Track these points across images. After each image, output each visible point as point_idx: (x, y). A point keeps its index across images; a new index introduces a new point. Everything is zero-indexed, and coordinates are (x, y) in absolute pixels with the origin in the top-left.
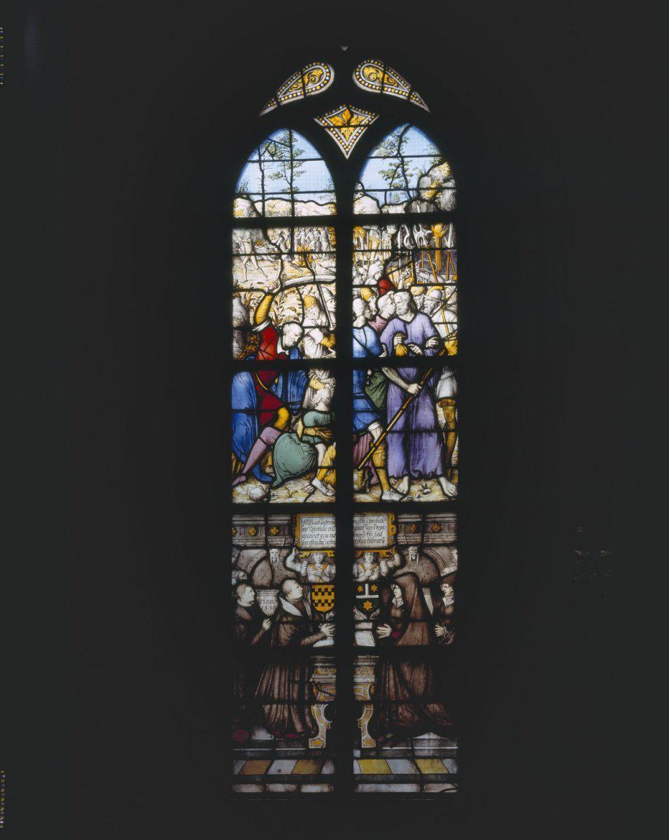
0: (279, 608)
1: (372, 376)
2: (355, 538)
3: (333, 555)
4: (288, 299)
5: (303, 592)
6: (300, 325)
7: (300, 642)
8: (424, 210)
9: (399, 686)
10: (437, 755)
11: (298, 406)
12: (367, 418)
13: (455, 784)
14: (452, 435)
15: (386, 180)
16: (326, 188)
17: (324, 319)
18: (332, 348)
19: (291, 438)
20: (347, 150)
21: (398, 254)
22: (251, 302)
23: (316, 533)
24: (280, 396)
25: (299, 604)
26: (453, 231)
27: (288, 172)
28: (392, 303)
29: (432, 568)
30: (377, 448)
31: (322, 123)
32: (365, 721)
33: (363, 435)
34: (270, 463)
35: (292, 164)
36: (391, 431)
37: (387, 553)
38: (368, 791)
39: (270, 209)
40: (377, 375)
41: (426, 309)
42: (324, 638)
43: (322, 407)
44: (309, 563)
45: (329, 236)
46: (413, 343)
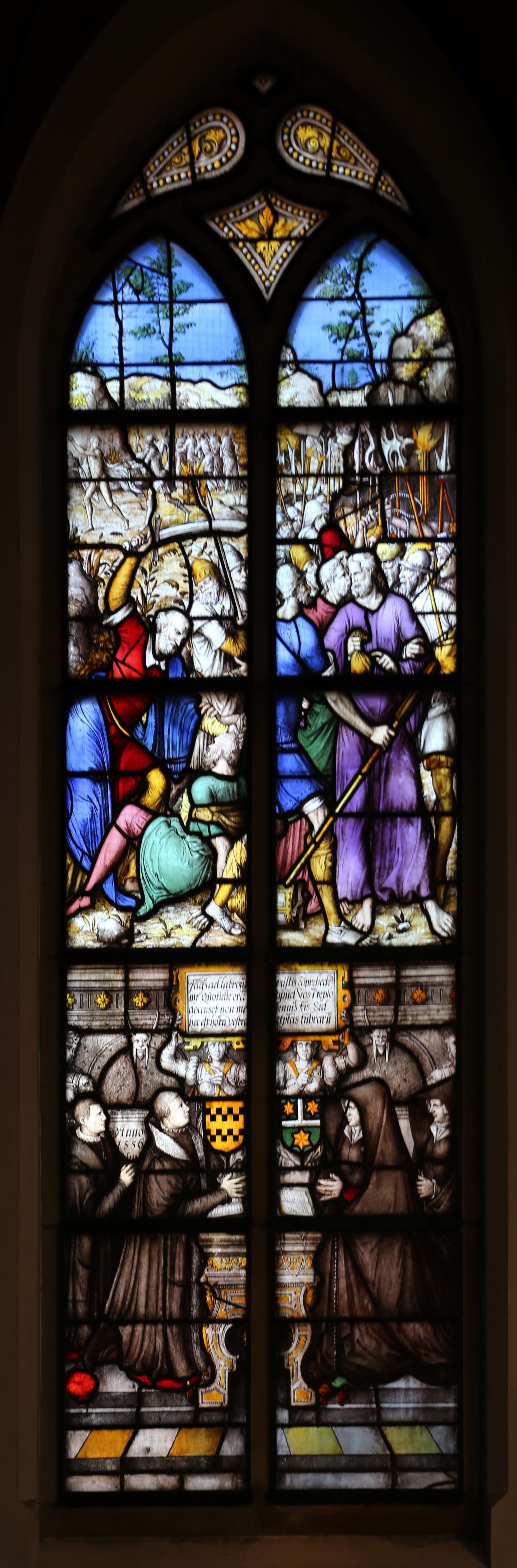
0: (149, 1142)
1: (310, 709)
2: (281, 1014)
3: (241, 1046)
4: (164, 565)
5: (191, 1115)
6: (186, 613)
7: (185, 1207)
8: (401, 399)
9: (355, 1290)
10: (421, 1419)
11: (183, 765)
12: (303, 788)
13: (452, 1474)
14: (446, 823)
15: (335, 341)
16: (232, 356)
17: (226, 603)
18: (240, 658)
19: (169, 825)
20: (267, 283)
21: (355, 483)
22: (101, 569)
23: (212, 1004)
24: (150, 748)
25: (182, 1136)
26: (450, 440)
27: (165, 325)
28: (344, 575)
29: (412, 1068)
30: (317, 846)
31: (225, 233)
32: (296, 1355)
33: (294, 822)
34: (132, 872)
35: (171, 309)
36: (343, 815)
37: (335, 1042)
38: (301, 1488)
39: (133, 394)
40: (318, 708)
41: (403, 586)
42: (227, 1200)
43: (222, 768)
44: (200, 1061)
45: (236, 446)
46: (379, 649)
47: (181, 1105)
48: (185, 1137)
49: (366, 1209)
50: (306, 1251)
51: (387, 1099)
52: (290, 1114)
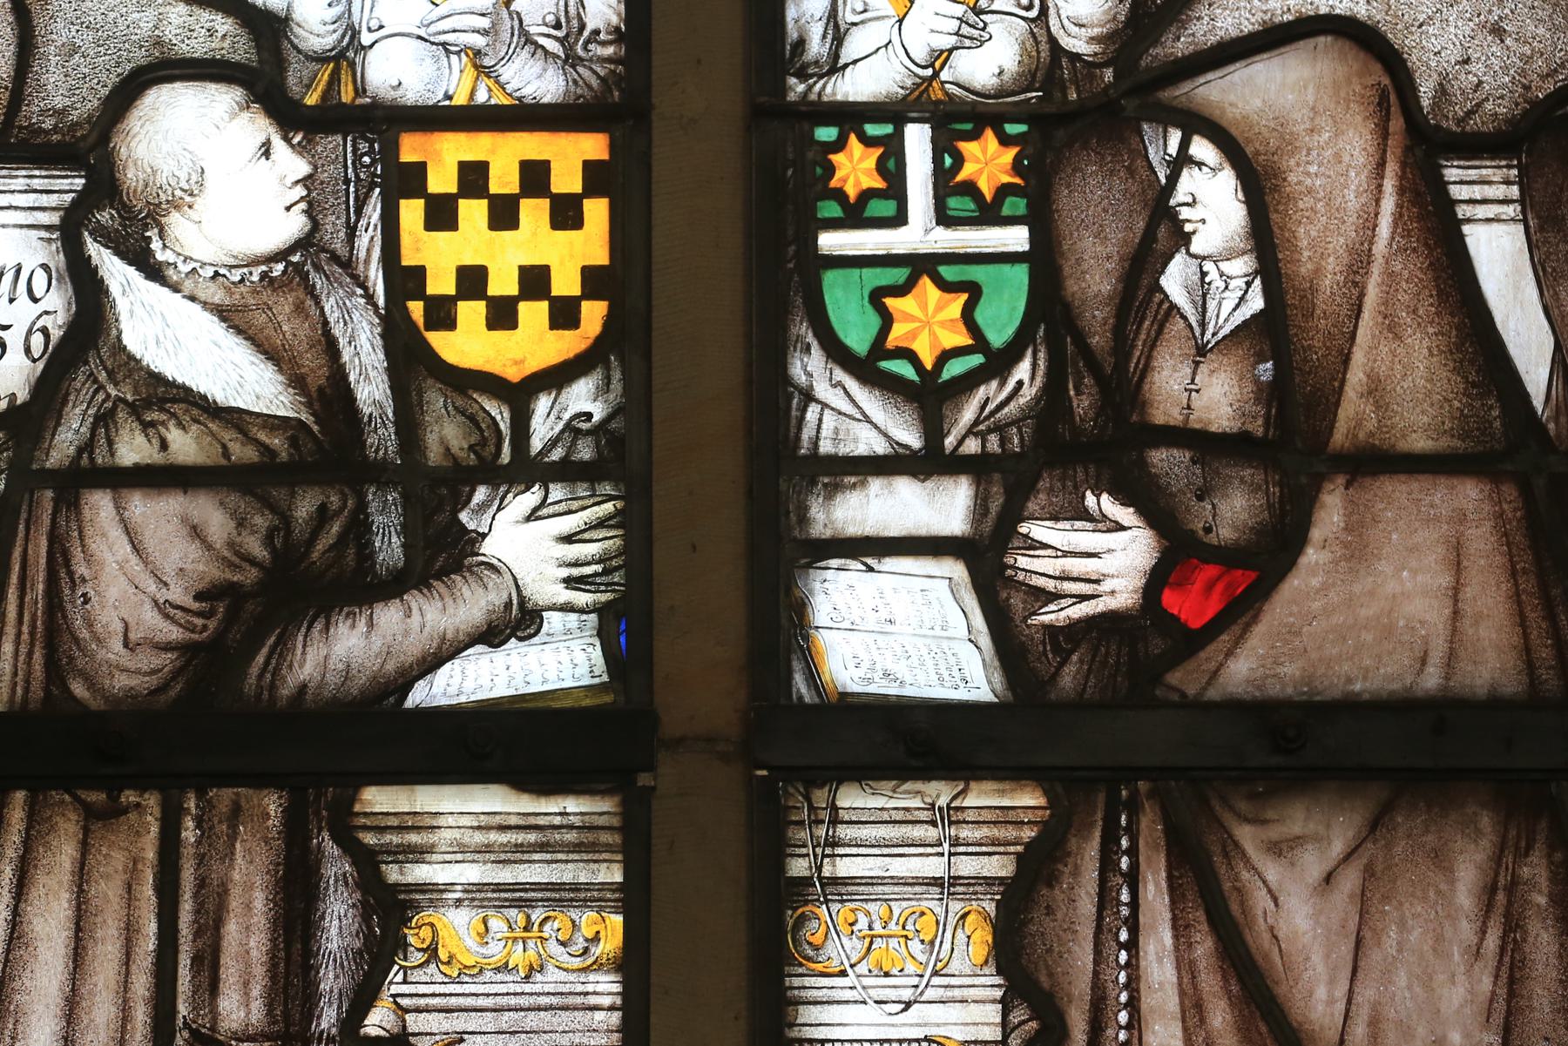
7: (282, 647)
47: (266, 150)
48: (284, 305)
49: (1290, 670)
50: (955, 880)
51: (1397, 124)
52: (867, 195)
